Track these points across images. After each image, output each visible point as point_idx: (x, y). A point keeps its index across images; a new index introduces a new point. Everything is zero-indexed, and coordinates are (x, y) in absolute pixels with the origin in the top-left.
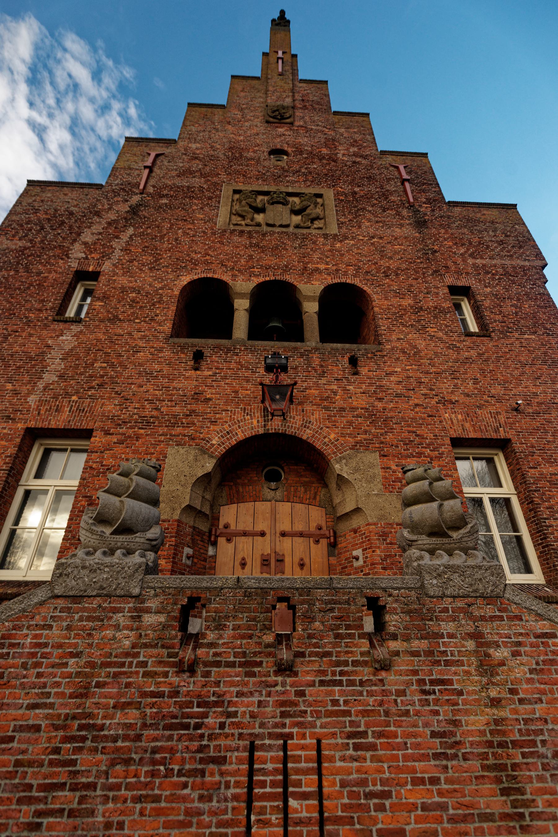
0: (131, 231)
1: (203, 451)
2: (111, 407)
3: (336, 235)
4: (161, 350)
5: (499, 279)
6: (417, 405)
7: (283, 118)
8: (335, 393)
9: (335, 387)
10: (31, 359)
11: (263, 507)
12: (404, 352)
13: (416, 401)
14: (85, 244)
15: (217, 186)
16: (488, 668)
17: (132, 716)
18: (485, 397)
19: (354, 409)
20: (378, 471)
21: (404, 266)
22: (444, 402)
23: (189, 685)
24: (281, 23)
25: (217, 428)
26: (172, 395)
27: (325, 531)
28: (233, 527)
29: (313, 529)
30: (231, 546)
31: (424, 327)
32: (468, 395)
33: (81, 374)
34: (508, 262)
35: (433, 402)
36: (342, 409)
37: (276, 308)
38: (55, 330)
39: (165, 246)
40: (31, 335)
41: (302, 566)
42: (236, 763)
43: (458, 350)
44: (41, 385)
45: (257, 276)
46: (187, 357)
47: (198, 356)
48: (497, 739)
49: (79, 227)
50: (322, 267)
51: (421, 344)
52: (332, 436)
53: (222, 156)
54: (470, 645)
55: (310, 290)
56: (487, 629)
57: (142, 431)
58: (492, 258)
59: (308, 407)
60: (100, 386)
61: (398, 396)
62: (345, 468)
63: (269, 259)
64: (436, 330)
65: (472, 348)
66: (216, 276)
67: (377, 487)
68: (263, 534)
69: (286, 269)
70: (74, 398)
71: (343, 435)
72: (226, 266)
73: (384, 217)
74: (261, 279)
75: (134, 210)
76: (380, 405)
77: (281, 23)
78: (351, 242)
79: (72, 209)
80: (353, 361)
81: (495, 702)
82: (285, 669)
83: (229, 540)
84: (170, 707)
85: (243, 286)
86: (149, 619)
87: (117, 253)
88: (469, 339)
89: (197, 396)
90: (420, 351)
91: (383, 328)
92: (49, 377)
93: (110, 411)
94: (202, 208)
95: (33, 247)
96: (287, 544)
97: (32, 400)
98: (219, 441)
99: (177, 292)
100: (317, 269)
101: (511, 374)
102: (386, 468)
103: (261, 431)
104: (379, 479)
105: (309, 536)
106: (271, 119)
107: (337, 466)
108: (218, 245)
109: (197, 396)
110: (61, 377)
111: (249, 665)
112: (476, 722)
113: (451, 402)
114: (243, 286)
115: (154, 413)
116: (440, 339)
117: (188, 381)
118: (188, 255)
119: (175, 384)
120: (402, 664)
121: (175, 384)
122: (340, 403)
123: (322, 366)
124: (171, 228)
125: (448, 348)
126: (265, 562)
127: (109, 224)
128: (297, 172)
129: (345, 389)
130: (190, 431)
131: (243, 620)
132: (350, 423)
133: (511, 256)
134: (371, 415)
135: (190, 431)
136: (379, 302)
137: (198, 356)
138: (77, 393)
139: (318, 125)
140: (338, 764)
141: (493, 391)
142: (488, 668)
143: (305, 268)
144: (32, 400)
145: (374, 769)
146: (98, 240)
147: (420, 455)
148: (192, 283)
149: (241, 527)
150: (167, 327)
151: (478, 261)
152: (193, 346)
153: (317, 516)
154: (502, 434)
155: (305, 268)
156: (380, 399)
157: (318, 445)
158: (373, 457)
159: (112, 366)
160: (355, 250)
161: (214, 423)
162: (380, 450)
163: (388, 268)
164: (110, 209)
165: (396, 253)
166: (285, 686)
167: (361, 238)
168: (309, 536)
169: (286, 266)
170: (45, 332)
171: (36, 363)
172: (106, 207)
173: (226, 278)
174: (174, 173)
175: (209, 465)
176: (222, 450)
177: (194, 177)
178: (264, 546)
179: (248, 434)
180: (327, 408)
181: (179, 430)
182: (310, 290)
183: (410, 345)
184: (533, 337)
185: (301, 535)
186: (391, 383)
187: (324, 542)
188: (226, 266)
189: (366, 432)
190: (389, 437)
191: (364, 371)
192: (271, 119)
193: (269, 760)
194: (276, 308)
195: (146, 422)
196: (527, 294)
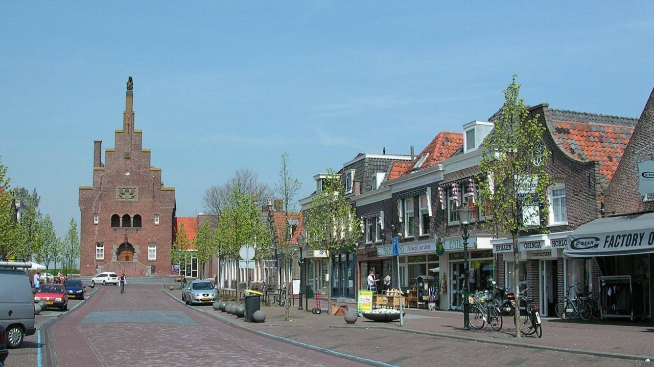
0: (101, 202)
1: (118, 245)
22: (149, 237)
24: (131, 79)
37: (127, 218)
47: (115, 230)
55: (132, 216)
63: (126, 209)
69: (128, 211)
75: (100, 197)
77: (131, 79)
85: (121, 216)
87: (100, 209)
89: (116, 237)
92: (96, 234)
98: (120, 244)
109: (116, 237)
114: (121, 216)
117: (114, 235)
134: (138, 239)
137: (115, 230)
148: (113, 215)
150: (110, 225)
158: (138, 245)
171: (94, 232)
175: (118, 247)
194: (127, 218)
195: (110, 241)
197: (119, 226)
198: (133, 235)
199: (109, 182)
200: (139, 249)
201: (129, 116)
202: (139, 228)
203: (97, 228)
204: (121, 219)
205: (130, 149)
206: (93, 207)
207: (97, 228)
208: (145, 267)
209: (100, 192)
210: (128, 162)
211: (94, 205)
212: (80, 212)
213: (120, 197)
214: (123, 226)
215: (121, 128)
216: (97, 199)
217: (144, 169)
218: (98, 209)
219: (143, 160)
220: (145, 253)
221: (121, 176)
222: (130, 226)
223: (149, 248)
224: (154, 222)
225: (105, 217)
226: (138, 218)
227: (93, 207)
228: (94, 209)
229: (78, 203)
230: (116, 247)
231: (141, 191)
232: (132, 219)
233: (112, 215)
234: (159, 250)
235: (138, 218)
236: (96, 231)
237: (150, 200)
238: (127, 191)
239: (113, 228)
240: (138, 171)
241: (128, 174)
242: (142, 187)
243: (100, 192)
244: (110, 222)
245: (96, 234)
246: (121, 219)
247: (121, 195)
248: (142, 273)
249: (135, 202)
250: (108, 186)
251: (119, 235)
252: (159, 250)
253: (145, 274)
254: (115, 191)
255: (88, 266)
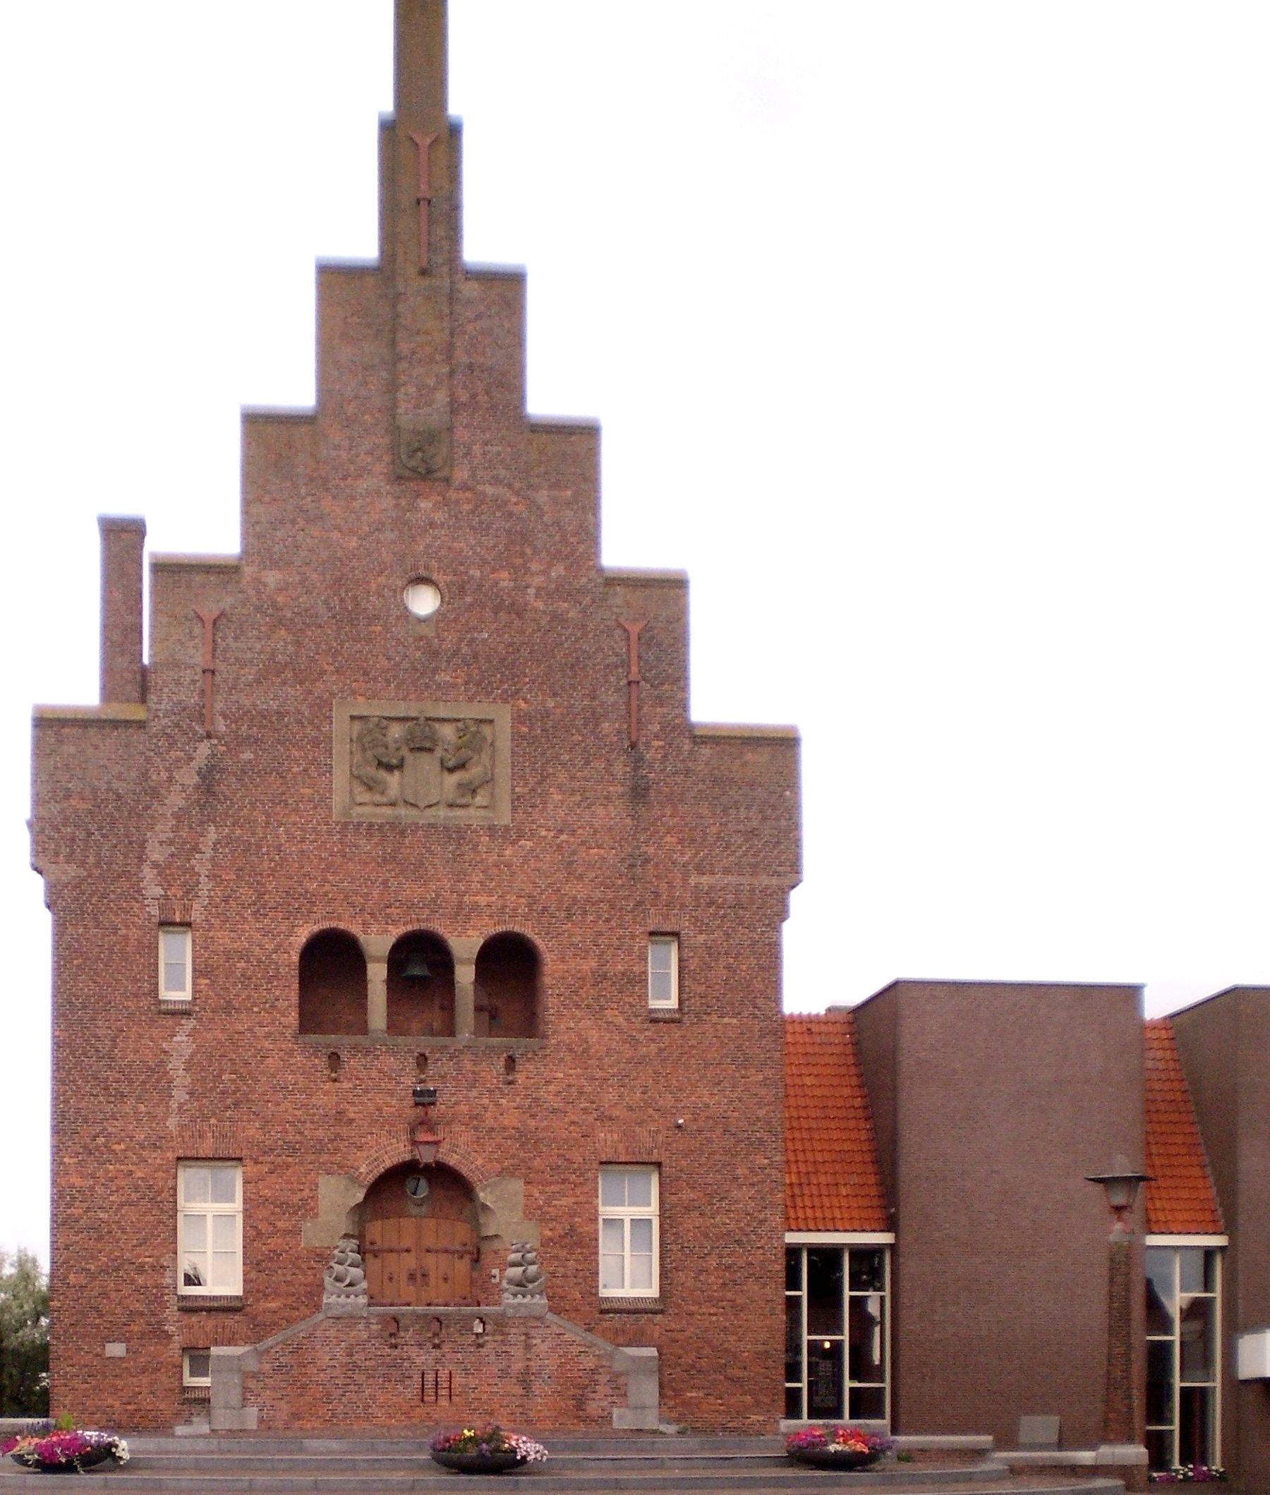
0: (212, 834)
1: (354, 1180)
2: (253, 1131)
3: (507, 829)
4: (291, 1053)
5: (724, 916)
6: (573, 1123)
7: (429, 472)
8: (486, 1109)
9: (486, 1101)
10: (149, 1068)
11: (408, 1224)
12: (571, 1050)
13: (573, 1118)
14: (155, 865)
15: (322, 707)
16: (528, 1347)
17: (372, 1363)
18: (651, 1111)
19: (505, 1129)
20: (521, 1199)
21: (598, 894)
23: (396, 1352)
25: (365, 1154)
26: (314, 1115)
27: (470, 1248)
28: (379, 1243)
29: (459, 1248)
30: (378, 1261)
31: (602, 1008)
32: (630, 1109)
33: (211, 1090)
34: (745, 880)
35: (591, 1119)
36: (492, 1129)
37: (421, 958)
38: (163, 1026)
39: (266, 865)
40: (141, 1036)
41: (445, 1279)
42: (417, 1378)
43: (634, 1043)
44: (174, 1105)
45: (394, 923)
46: (321, 1062)
47: (335, 1059)
48: (527, 1371)
49: (138, 828)
50: (483, 900)
51: (594, 1036)
52: (480, 1162)
53: (322, 610)
54: (523, 1338)
55: (465, 946)
56: (533, 1332)
57: (290, 1159)
58: (727, 871)
59: (457, 1128)
60: (236, 1104)
61: (554, 1111)
62: (489, 1196)
63: (412, 890)
64: (616, 1012)
65: (653, 1040)
66: (342, 926)
67: (518, 1215)
68: (408, 1251)
69: (434, 905)
70: (213, 1121)
71: (490, 1160)
72: (352, 905)
73: (585, 779)
74: (401, 930)
75: (209, 779)
76: (532, 1123)
78: (529, 844)
79: (116, 784)
80: (511, 1063)
81: (528, 1359)
82: (436, 1346)
83: (376, 1256)
84: (388, 1360)
85: (378, 943)
86: (374, 1327)
87: (205, 886)
88: (653, 1027)
90: (589, 1048)
91: (552, 1011)
92: (180, 1095)
93: (253, 1136)
94: (305, 770)
95: (90, 876)
96: (430, 1260)
97: (172, 1123)
98: (368, 1170)
99: (295, 958)
100: (475, 907)
101: (689, 1079)
102: (528, 1196)
103: (408, 1157)
104: (520, 1208)
105: (453, 1252)
106: (407, 473)
107: (481, 1195)
108: (339, 860)
110: (191, 1094)
111: (420, 1345)
112: (518, 1366)
113: (611, 1119)
114: (378, 943)
115: (298, 1138)
116: (618, 1027)
117: (325, 1098)
118: (300, 883)
119: (314, 1100)
120: (489, 1346)
121: (314, 1100)
122: (490, 1122)
123: (474, 1073)
124: (267, 823)
125: (624, 1042)
126: (412, 1277)
127: (176, 816)
128: (454, 656)
129: (497, 1105)
130: (338, 1158)
131: (417, 1327)
132: (499, 1146)
133: (754, 866)
134: (522, 1136)
135: (338, 1158)
136: (553, 966)
137: (335, 1059)
138: (214, 1114)
139: (496, 481)
140: (458, 1380)
141: (661, 1103)
142: (528, 1347)
143: (460, 906)
144: (172, 1123)
145: (472, 1382)
146: (172, 855)
147: (564, 1181)
149: (386, 1246)
150: (293, 1018)
151: (705, 879)
152: (328, 1046)
153: (460, 1233)
154: (654, 1158)
155: (460, 906)
156: (533, 1116)
157: (464, 1171)
158: (517, 1185)
159: (242, 1078)
160: (532, 864)
161: (360, 1148)
162: (526, 1176)
163: (574, 898)
164: (170, 779)
165: (591, 866)
166: (437, 1353)
167: (544, 833)
168: (453, 1252)
169: (434, 901)
170: (155, 1032)
171: (157, 1075)
172: (164, 775)
173: (355, 929)
174: (249, 674)
175: (360, 1196)
176: (371, 1178)
177: (284, 683)
178: (410, 1261)
179: (396, 1161)
180: (476, 1129)
181: (325, 1157)
182: (465, 946)
183: (580, 1036)
184: (735, 1021)
185: (446, 1251)
186: (548, 1095)
187: (467, 1258)
188: (352, 905)
189: (513, 1156)
190: (537, 1162)
191: (520, 1078)
192: (407, 473)
193: (430, 1378)
194: (421, 958)
195: (293, 1149)
196: (754, 943)
197: (363, 1029)
198: (483, 1100)
199: (272, 670)
200: (528, 1214)
201: (420, 154)
202: (519, 1045)
203: (182, 1042)
204: (377, 973)
205: (441, 397)
206: (148, 873)
207: (182, 1042)
208: (611, 1357)
209: (204, 749)
210: (425, 504)
211: (156, 853)
212: (46, 918)
213: (370, 785)
214: (393, 1027)
215: (361, 242)
216: (176, 800)
217: (558, 570)
218: (190, 891)
219: (542, 496)
220: (576, 1244)
221: (372, 619)
222: (450, 1031)
223: (607, 1211)
224: (644, 997)
225: (244, 955)
226: (510, 961)
227: (148, 873)
228: (154, 891)
229: (23, 842)
230: (336, 1197)
231: (536, 736)
232: (465, 975)
233: (302, 935)
234: (691, 1222)
235: (510, 961)
236: (176, 1066)
237: (611, 815)
238: (422, 745)
239: (312, 1038)
240: (504, 579)
241: (424, 602)
242: (547, 715)
243: (204, 749)
244: (291, 995)
245: (180, 1095)
246: (377, 973)
247: (371, 771)
248: (580, 1403)
249: (492, 830)
250: (266, 700)
251: (370, 1096)
252: (691, 1222)
253: (608, 1419)
254: (323, 743)
255: (116, 1349)
